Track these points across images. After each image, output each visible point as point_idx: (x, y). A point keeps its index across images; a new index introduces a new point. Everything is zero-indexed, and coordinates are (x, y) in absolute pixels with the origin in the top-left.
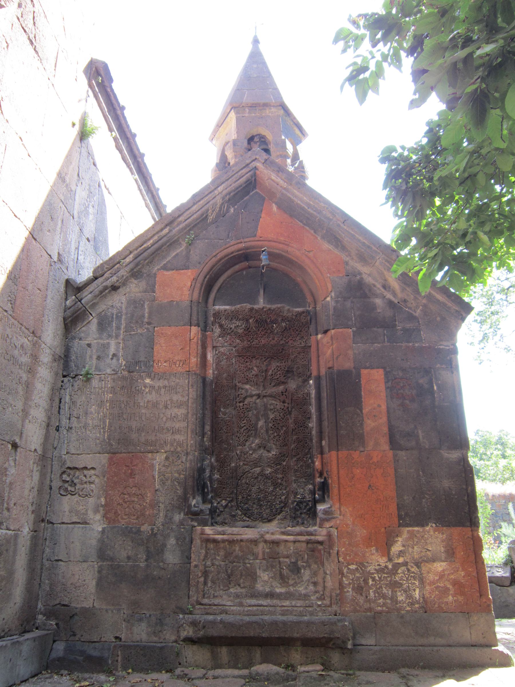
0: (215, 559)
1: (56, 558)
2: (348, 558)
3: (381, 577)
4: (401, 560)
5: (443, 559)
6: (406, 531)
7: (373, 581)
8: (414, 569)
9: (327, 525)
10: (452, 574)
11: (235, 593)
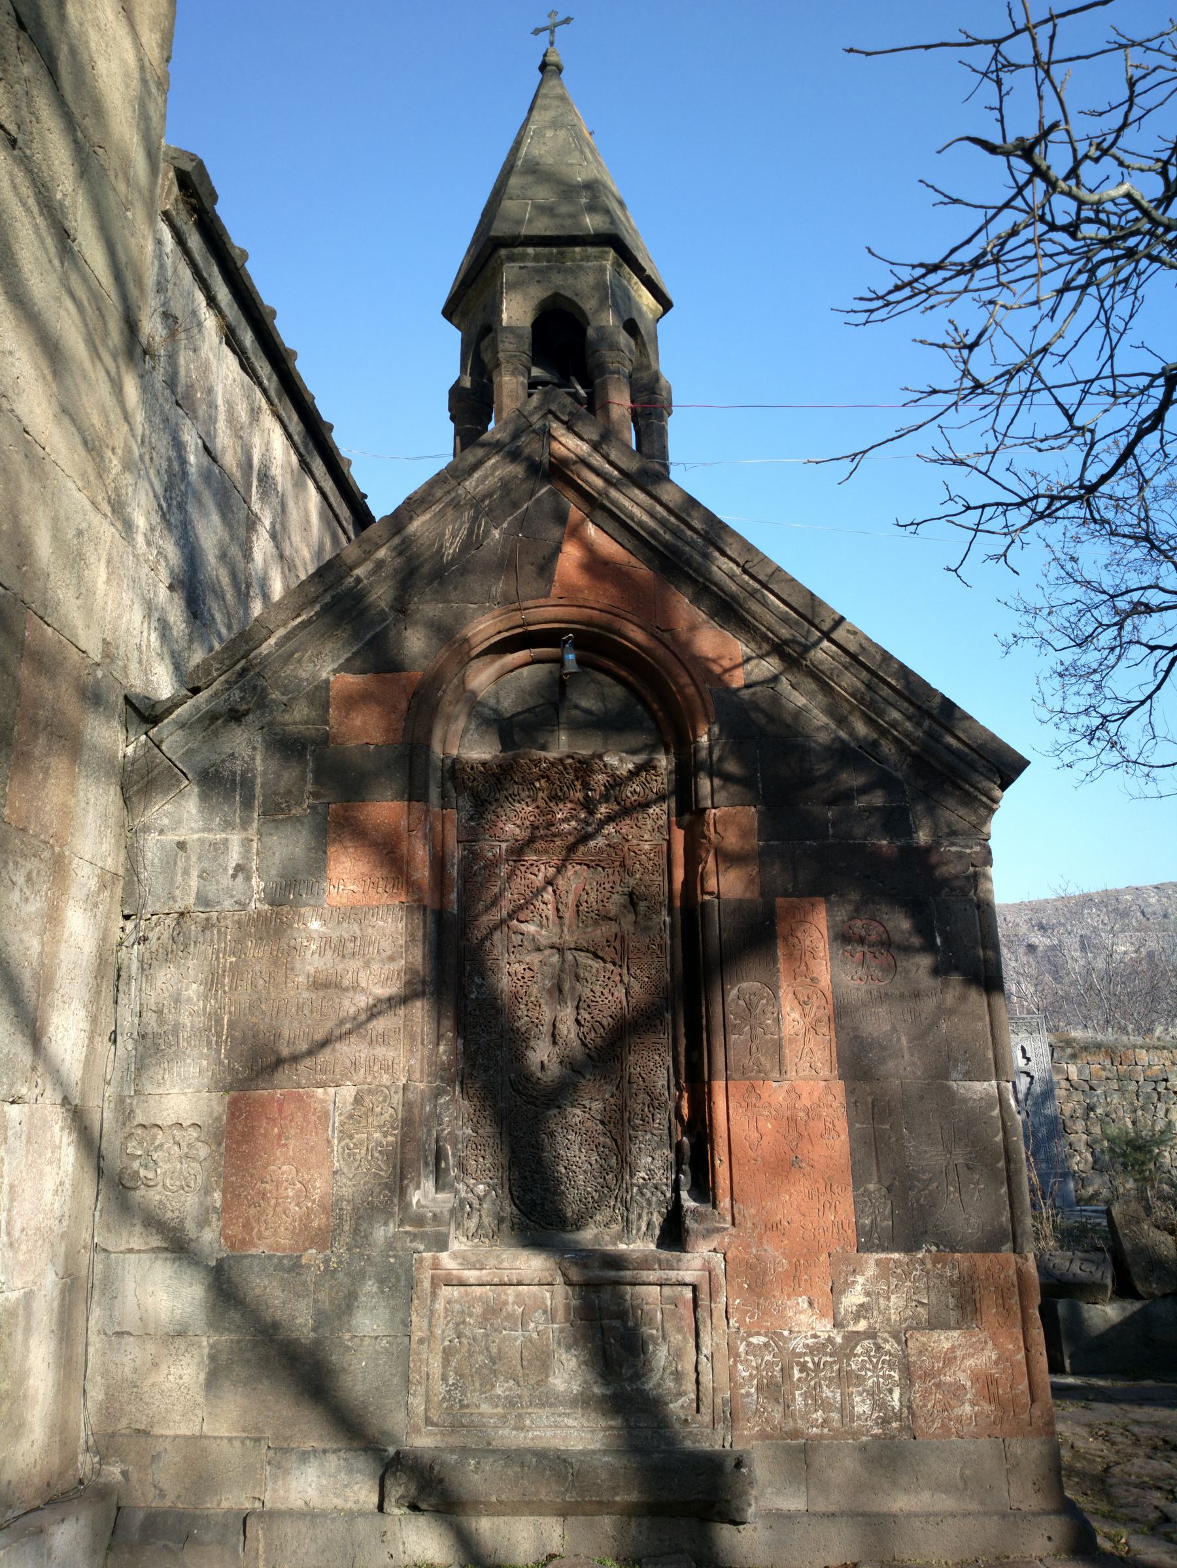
0: (464, 1322)
1: (118, 1329)
4: (862, 1325)
5: (953, 1323)
6: (872, 1262)
7: (801, 1371)
8: (890, 1346)
10: (971, 1355)
11: (506, 1397)
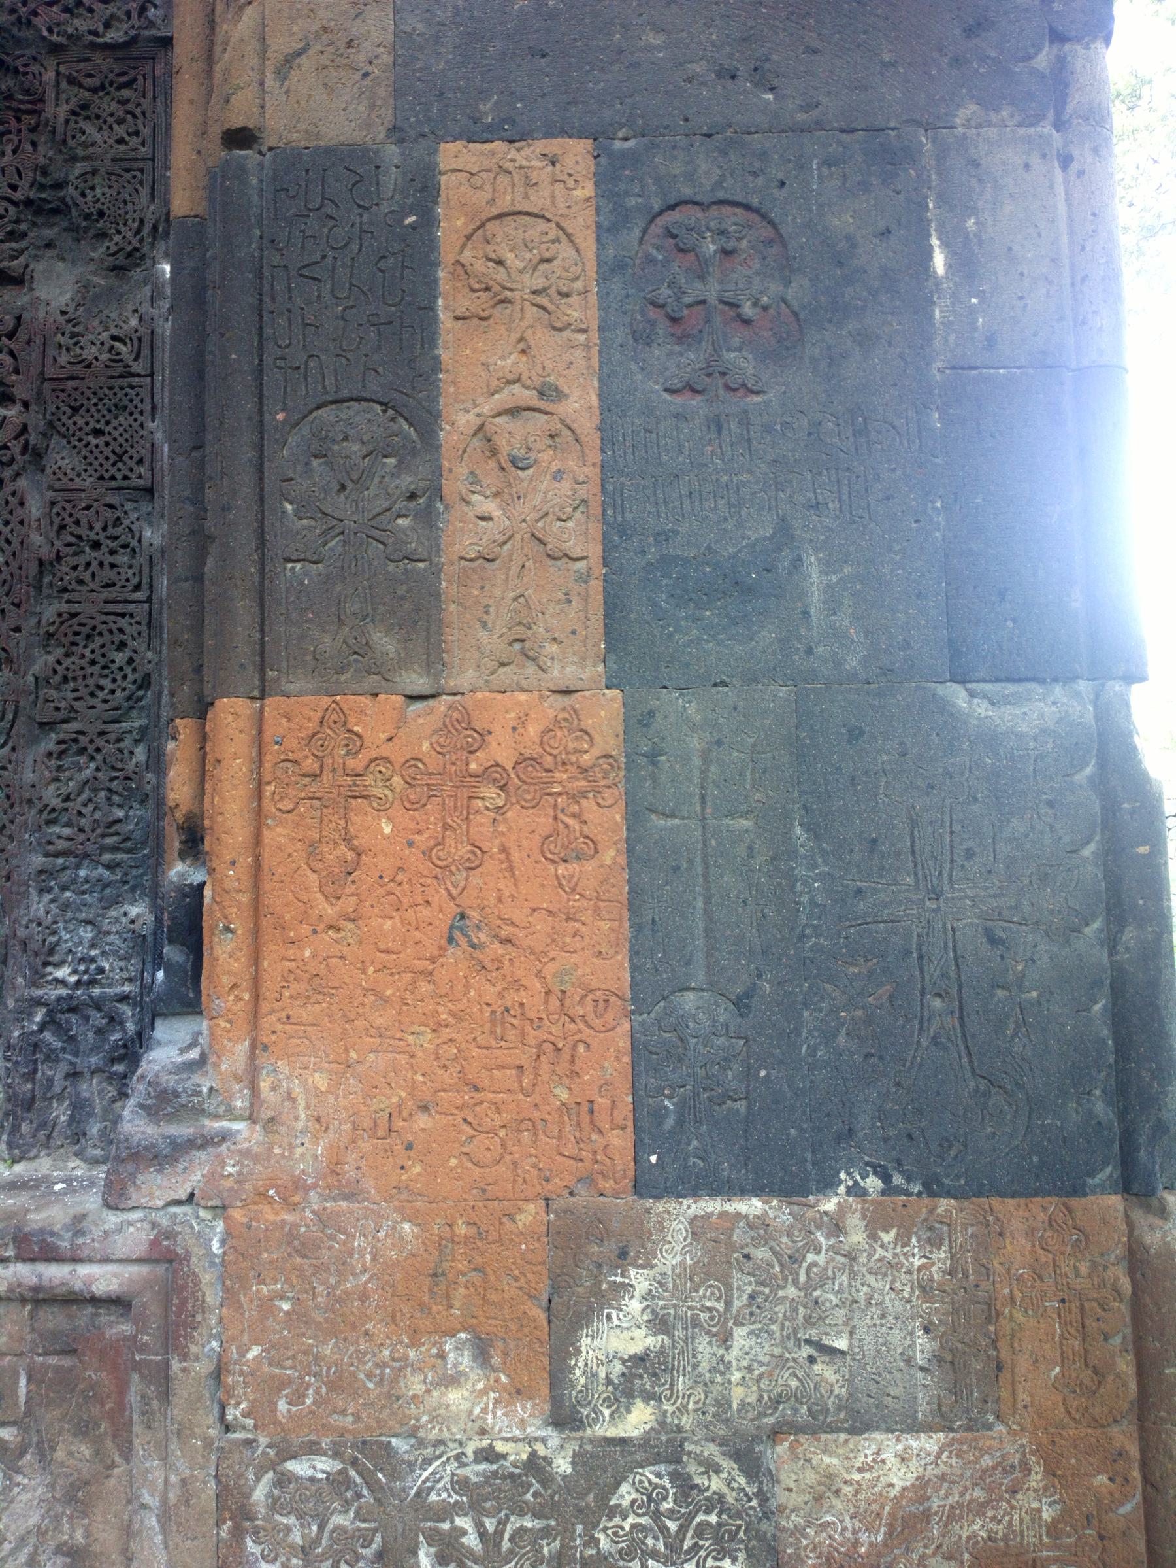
2: (282, 1406)
3: (499, 1533)
4: (638, 1420)
6: (679, 1229)
9: (157, 1188)
10: (980, 1509)
